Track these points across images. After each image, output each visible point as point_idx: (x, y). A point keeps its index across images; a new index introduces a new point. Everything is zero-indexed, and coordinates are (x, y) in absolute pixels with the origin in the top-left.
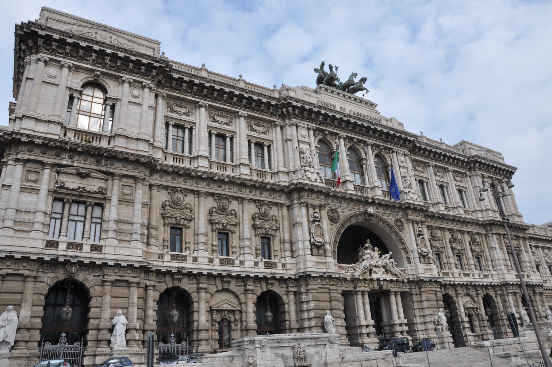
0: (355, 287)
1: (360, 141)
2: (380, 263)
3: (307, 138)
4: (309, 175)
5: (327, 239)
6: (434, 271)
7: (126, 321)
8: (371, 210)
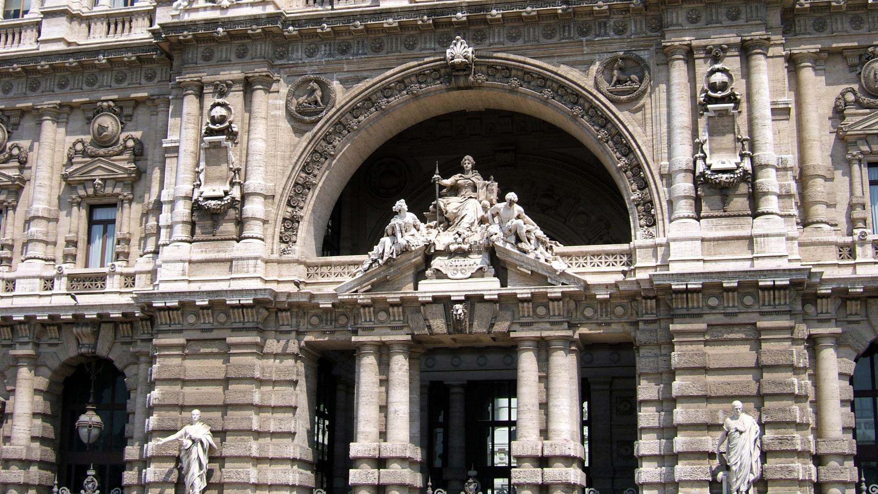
2: (477, 237)
6: (777, 245)
8: (460, 50)
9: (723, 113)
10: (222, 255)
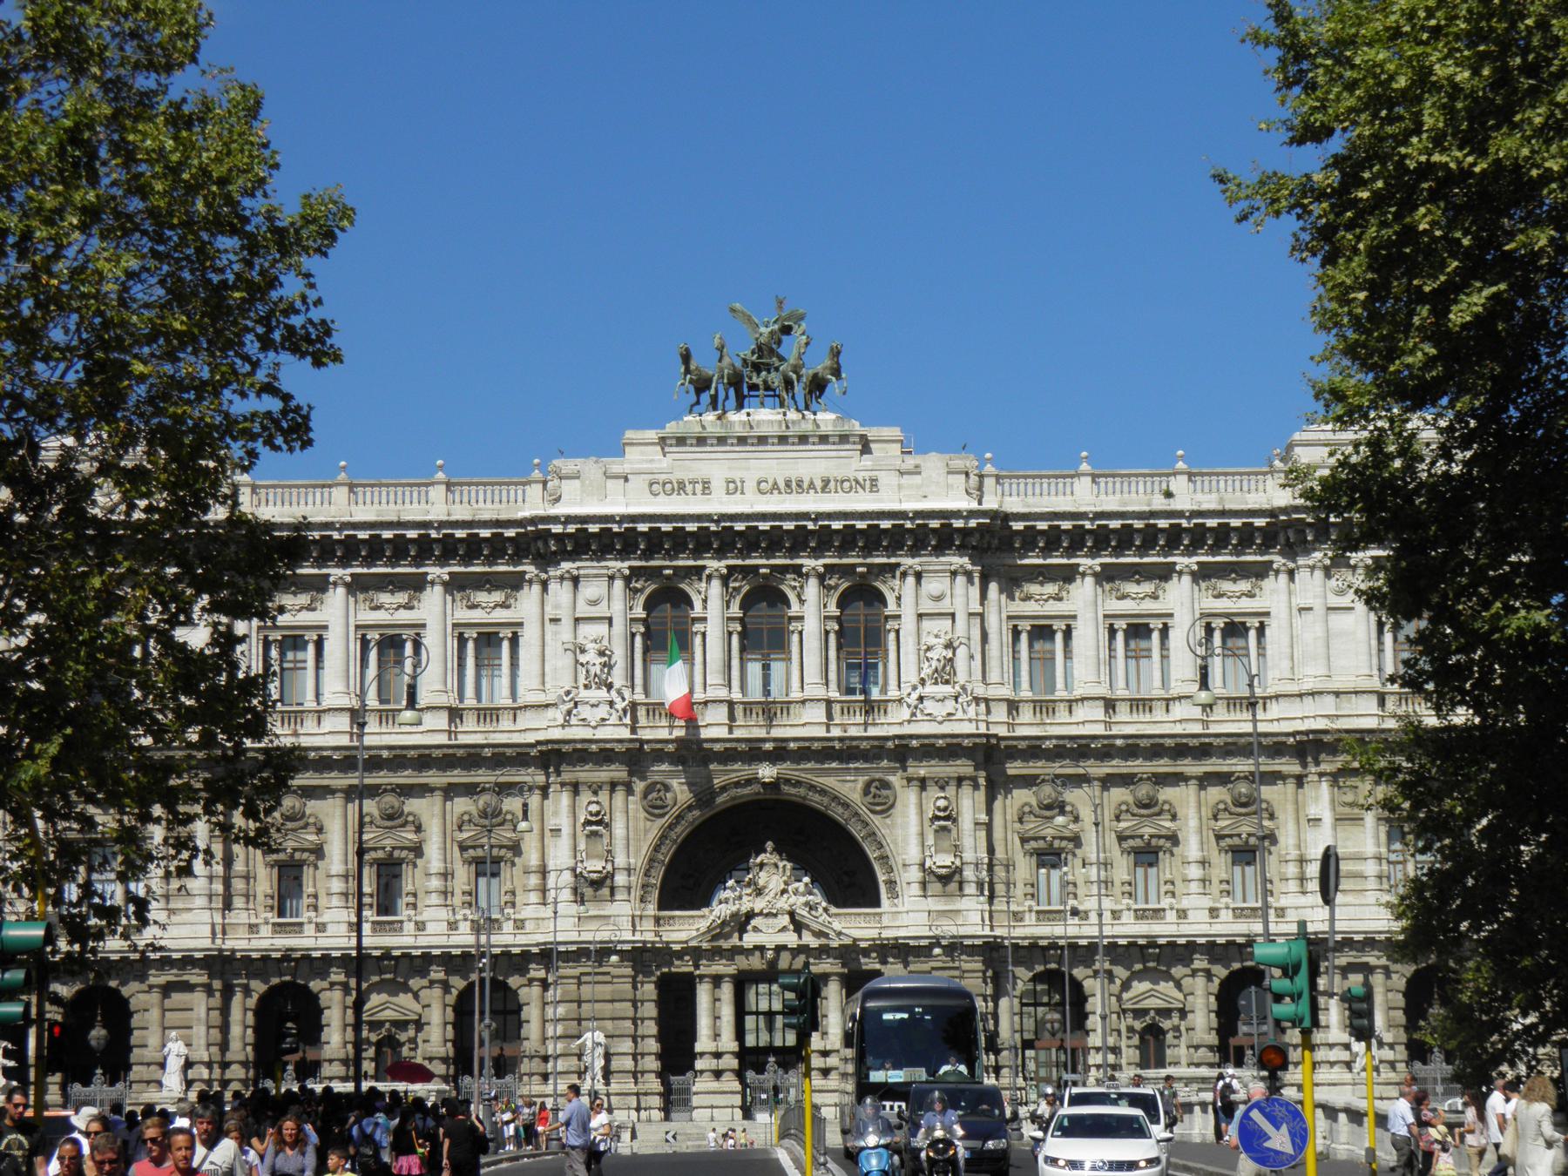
0: (697, 967)
1: (784, 569)
2: (783, 903)
3: (605, 602)
4: (585, 711)
5: (620, 861)
7: (184, 1050)
8: (767, 772)
9: (944, 828)
10: (602, 913)
